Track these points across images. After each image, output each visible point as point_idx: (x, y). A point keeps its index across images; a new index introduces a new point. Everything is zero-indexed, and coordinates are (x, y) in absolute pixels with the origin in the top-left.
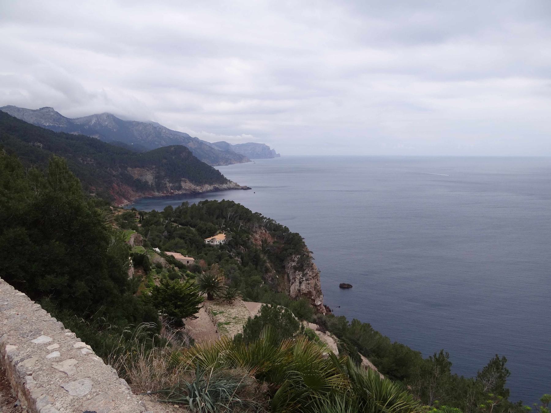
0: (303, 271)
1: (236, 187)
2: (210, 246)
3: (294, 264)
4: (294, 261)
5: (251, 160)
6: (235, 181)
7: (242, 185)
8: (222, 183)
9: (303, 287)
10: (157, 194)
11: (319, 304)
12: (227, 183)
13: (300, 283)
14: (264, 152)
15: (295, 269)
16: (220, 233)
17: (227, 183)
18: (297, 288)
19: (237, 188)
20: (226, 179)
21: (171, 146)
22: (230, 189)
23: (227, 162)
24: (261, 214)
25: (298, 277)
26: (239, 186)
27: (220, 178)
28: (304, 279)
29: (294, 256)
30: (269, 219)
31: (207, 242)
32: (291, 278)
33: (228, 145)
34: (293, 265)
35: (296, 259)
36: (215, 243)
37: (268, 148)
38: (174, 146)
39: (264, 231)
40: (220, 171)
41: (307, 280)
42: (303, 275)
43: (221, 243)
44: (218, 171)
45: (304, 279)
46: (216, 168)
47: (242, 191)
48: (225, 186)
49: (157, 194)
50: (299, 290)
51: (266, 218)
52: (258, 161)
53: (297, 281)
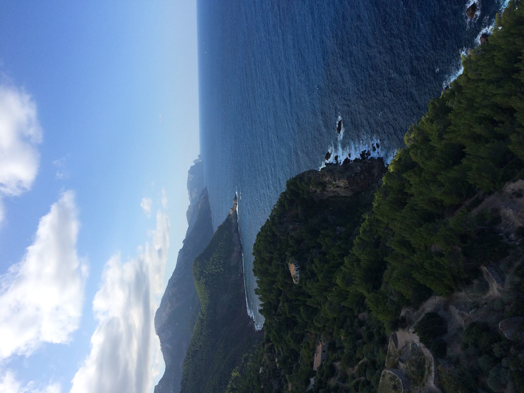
0: (325, 182)
2: (301, 281)
3: (318, 191)
4: (316, 191)
5: (205, 186)
9: (342, 185)
11: (359, 169)
12: (231, 219)
13: (338, 187)
15: (324, 189)
16: (287, 265)
17: (231, 219)
18: (342, 190)
20: (228, 220)
24: (268, 220)
25: (332, 188)
28: (334, 183)
29: (310, 191)
30: (272, 211)
31: (297, 283)
32: (332, 194)
34: (319, 192)
35: (314, 189)
36: (298, 275)
39: (285, 219)
41: (335, 181)
42: (331, 183)
43: (298, 269)
45: (334, 183)
46: (215, 229)
50: (346, 188)
51: (271, 214)
53: (336, 189)
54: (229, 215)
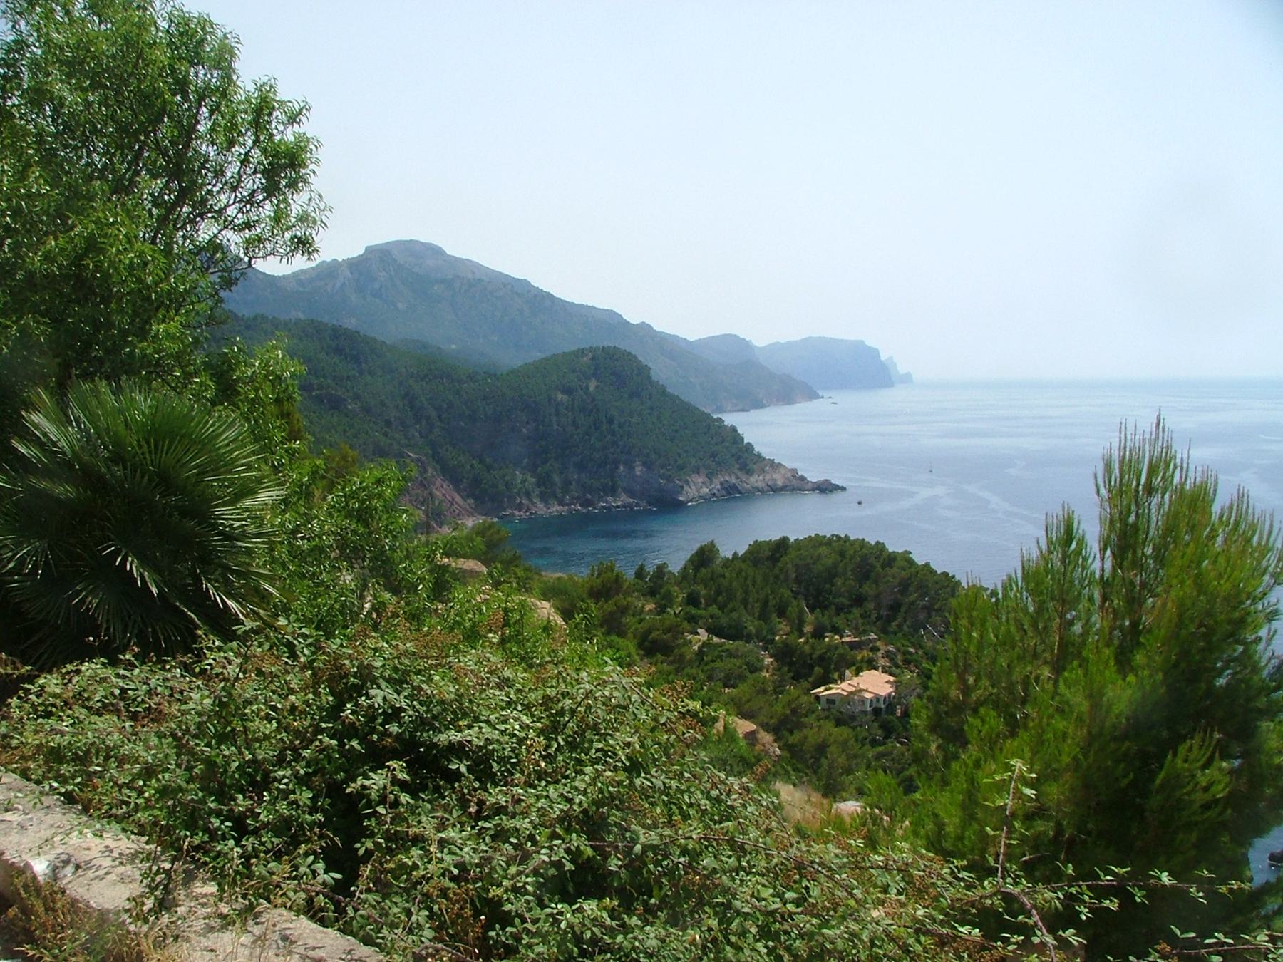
1: (794, 482)
6: (789, 465)
7: (813, 477)
8: (749, 473)
10: (541, 509)
14: (862, 369)
19: (796, 485)
21: (581, 353)
22: (775, 490)
23: (752, 402)
26: (803, 479)
27: (741, 456)
33: (745, 345)
37: (874, 353)
38: (591, 349)
40: (740, 431)
44: (734, 429)
46: (729, 419)
47: (814, 499)
48: (756, 480)
49: (541, 509)
52: (847, 400)
54: (774, 465)
